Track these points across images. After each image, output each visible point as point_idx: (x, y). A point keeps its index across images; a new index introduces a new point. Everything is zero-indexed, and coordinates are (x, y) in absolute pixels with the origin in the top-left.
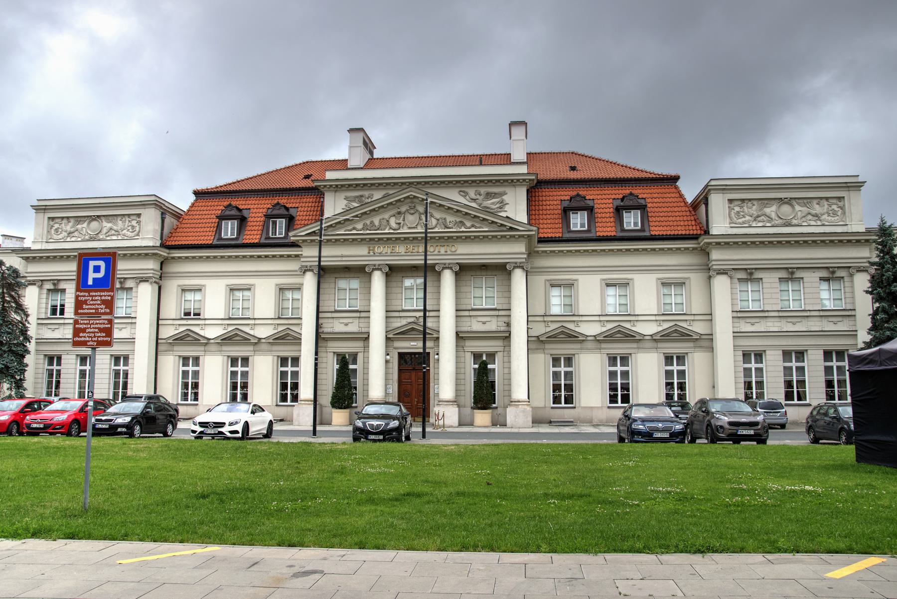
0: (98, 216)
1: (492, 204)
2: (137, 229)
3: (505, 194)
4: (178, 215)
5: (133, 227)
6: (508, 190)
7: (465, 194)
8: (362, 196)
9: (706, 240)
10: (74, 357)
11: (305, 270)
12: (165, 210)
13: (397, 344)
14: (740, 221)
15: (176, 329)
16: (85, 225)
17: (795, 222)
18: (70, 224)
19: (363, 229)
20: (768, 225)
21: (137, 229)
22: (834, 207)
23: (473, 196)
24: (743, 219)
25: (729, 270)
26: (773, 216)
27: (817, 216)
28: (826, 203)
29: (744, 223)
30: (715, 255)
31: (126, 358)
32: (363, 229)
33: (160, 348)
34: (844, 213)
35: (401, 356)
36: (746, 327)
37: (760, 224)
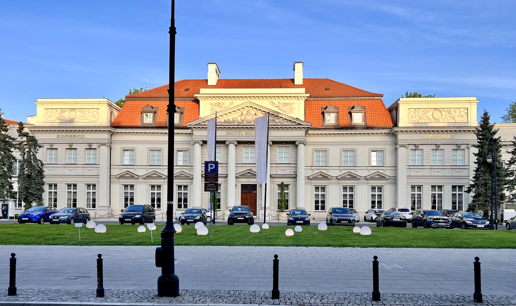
1: (287, 109)
2: (97, 116)
3: (292, 104)
5: (95, 115)
8: (220, 103)
9: (396, 129)
13: (241, 180)
15: (121, 170)
18: (58, 113)
21: (97, 116)
23: (277, 105)
25: (406, 145)
30: (400, 137)
31: (94, 186)
32: (224, 122)
33: (111, 181)
35: (243, 186)
36: (413, 173)
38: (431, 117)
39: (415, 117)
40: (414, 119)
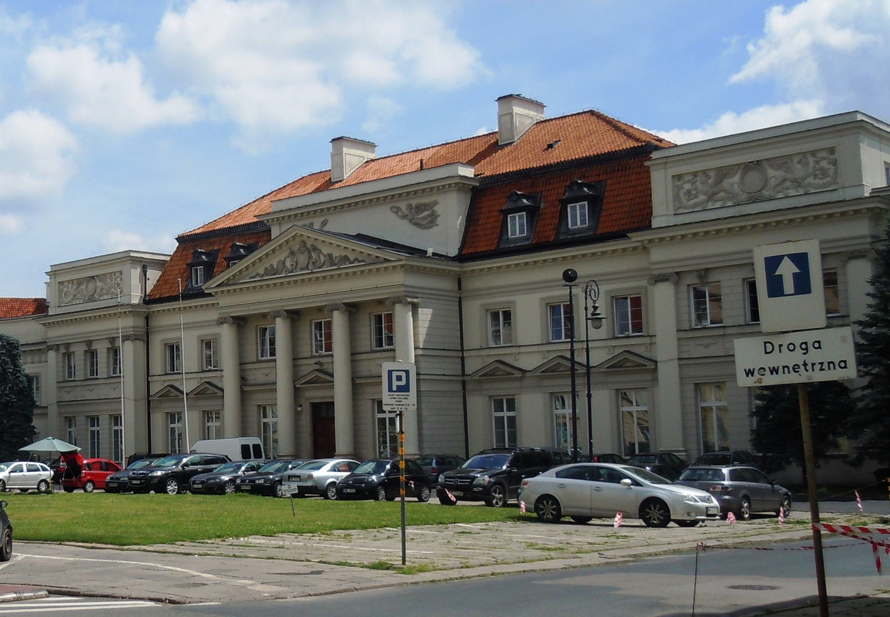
1: (424, 218)
3: (436, 203)
4: (159, 264)
5: (118, 285)
6: (439, 198)
7: (397, 210)
9: (637, 238)
10: (84, 418)
11: (221, 322)
12: (145, 264)
14: (692, 202)
16: (84, 287)
17: (766, 193)
19: (266, 274)
20: (730, 203)
22: (824, 164)
24: (695, 201)
25: (670, 275)
26: (736, 189)
27: (798, 183)
28: (811, 160)
29: (695, 206)
34: (836, 173)
37: (718, 205)
38: (736, 189)
39: (696, 196)
40: (692, 202)
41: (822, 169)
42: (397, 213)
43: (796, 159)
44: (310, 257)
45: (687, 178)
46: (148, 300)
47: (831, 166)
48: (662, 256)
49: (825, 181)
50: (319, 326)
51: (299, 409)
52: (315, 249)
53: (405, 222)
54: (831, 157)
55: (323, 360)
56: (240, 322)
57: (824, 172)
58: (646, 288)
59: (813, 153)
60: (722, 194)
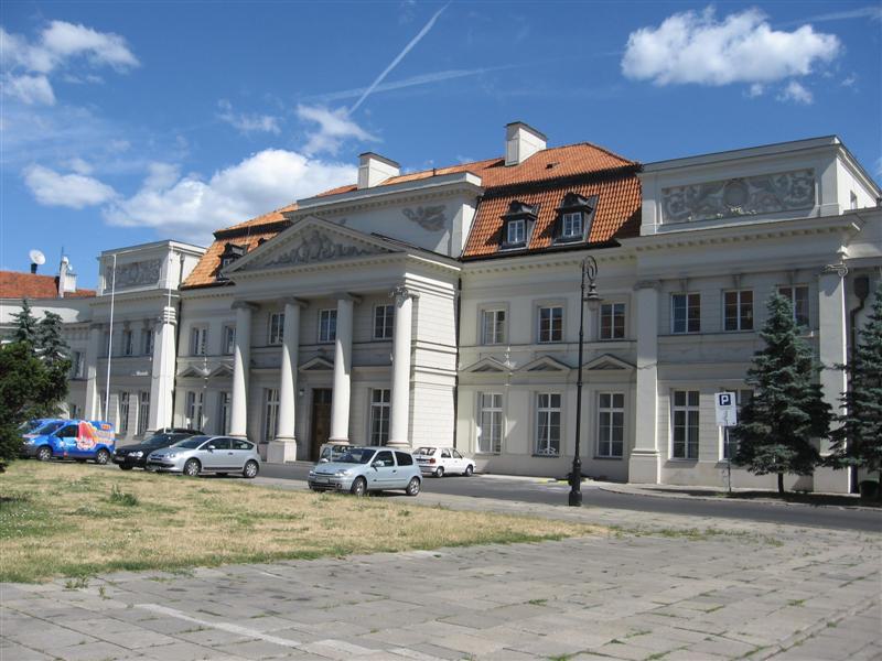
0: (136, 264)
3: (444, 207)
7: (408, 212)
28: (790, 179)
29: (681, 217)
39: (682, 209)
41: (800, 188)
42: (408, 215)
43: (776, 179)
44: (322, 247)
45: (674, 192)
46: (183, 288)
47: (808, 186)
48: (648, 263)
49: (803, 199)
50: (325, 315)
51: (301, 393)
52: (326, 239)
53: (415, 223)
54: (809, 177)
55: (325, 348)
56: (255, 307)
57: (802, 192)
58: (630, 295)
59: (792, 173)
60: (706, 208)
